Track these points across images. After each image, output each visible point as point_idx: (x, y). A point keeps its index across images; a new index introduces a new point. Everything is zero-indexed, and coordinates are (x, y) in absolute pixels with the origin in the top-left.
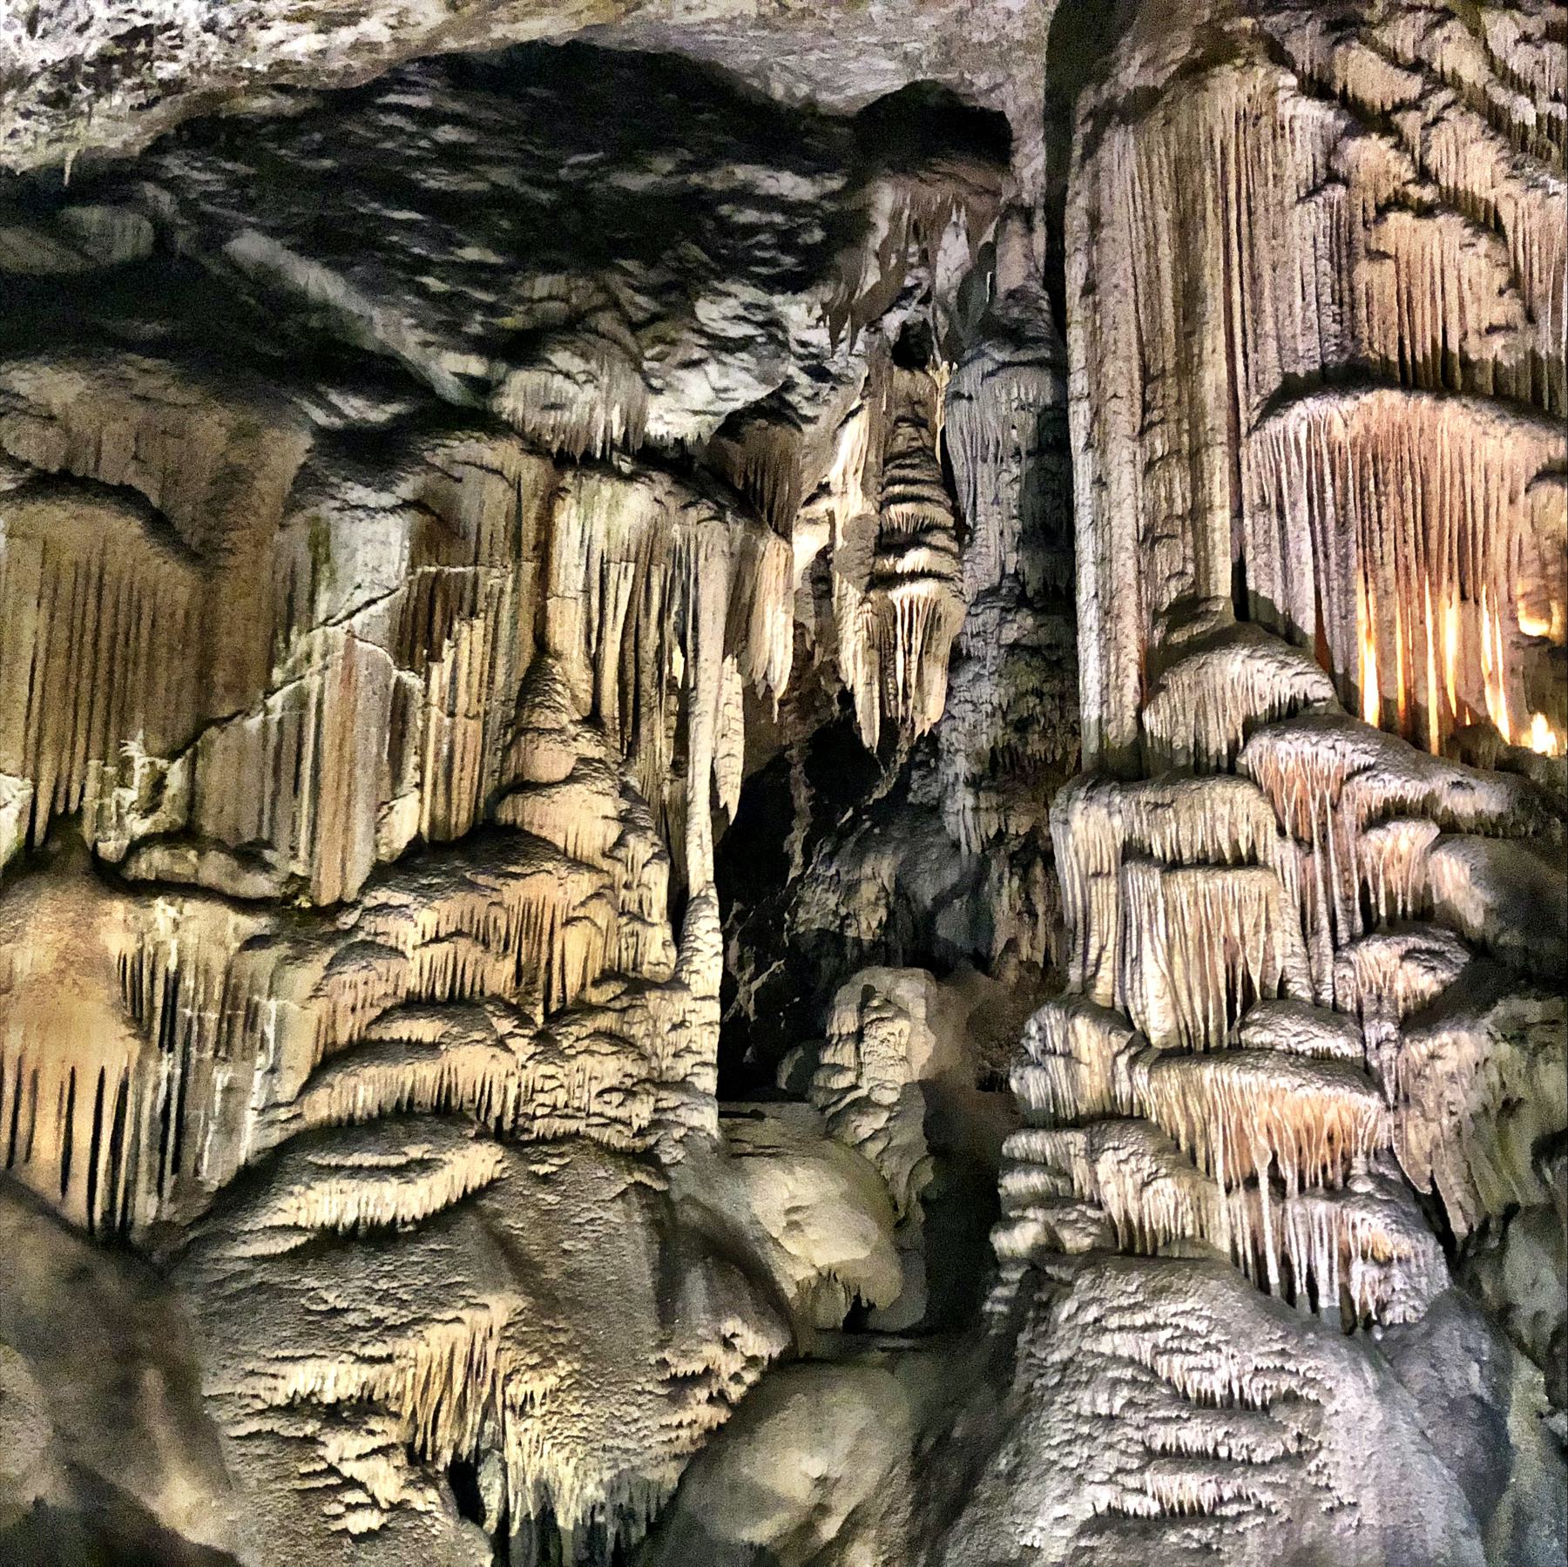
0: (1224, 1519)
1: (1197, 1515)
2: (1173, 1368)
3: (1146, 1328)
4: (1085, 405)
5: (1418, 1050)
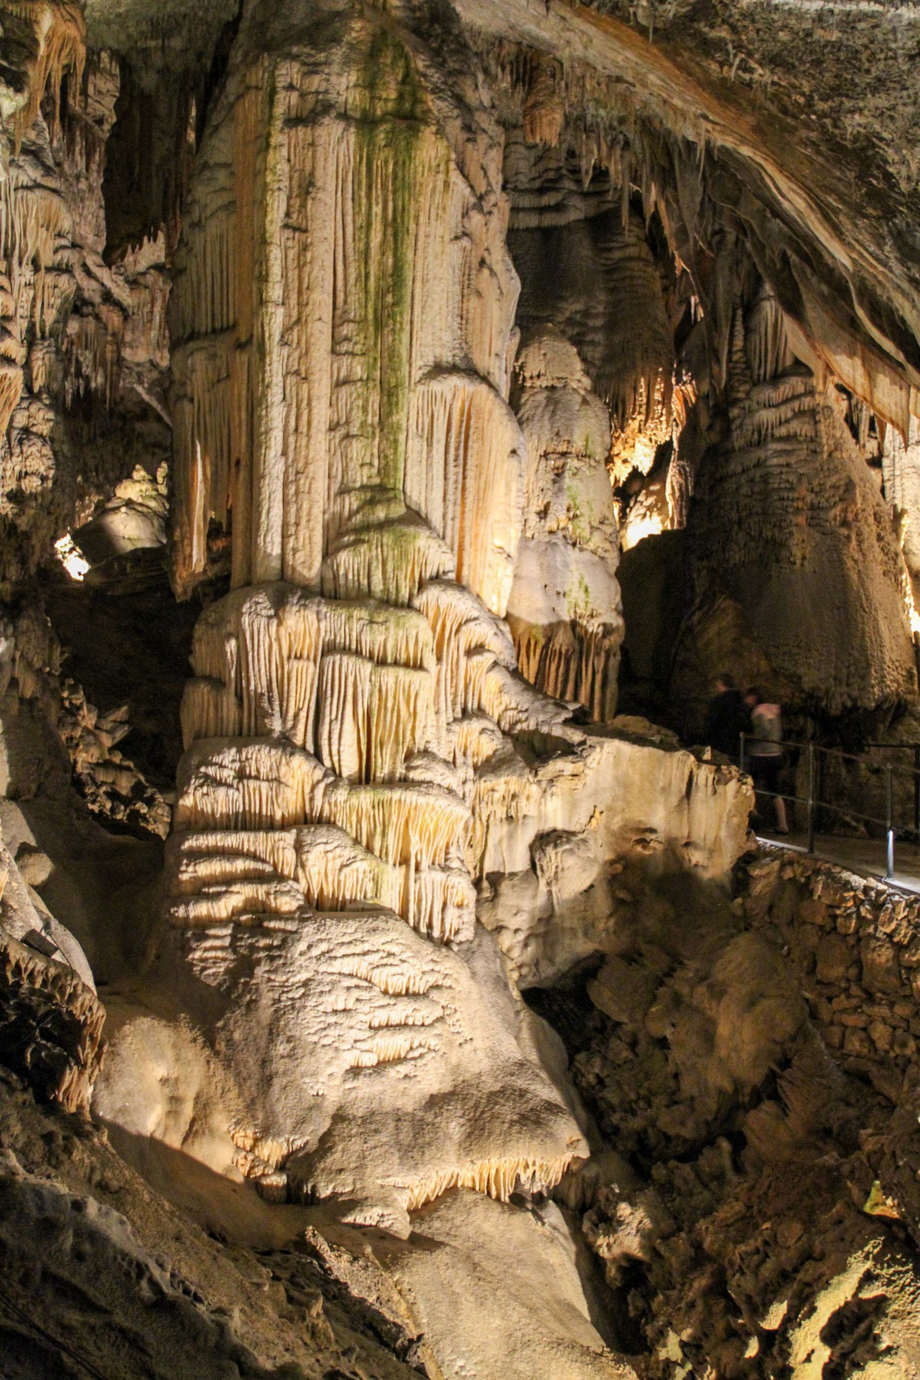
0: (414, 1059)
1: (400, 1060)
2: (380, 977)
3: (365, 954)
4: (281, 311)
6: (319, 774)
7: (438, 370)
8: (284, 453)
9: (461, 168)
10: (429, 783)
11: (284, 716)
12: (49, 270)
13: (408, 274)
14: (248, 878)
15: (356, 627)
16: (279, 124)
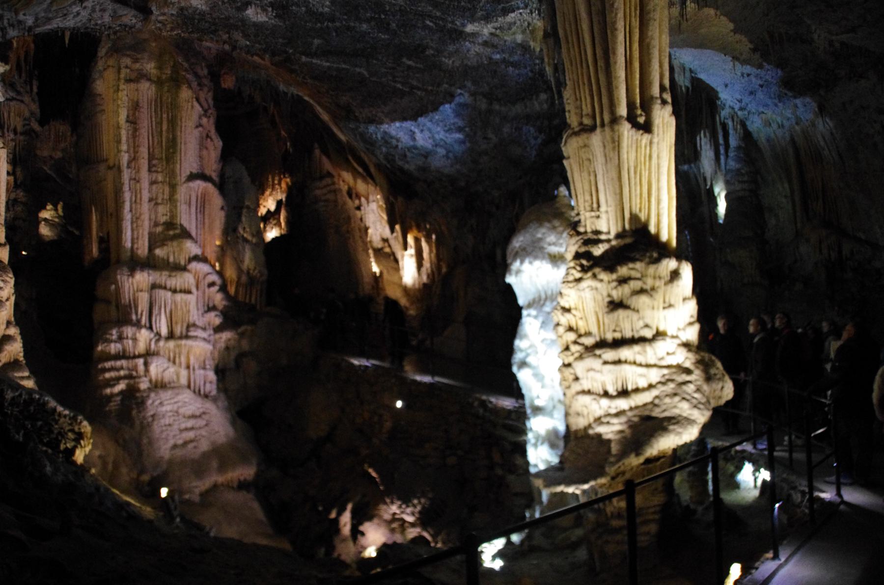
1: (191, 441)
3: (176, 403)
4: (127, 155)
5: (218, 336)
6: (152, 335)
7: (192, 177)
8: (131, 211)
9: (198, 100)
10: (196, 337)
11: (137, 314)
12: (21, 134)
13: (179, 141)
14: (125, 377)
15: (164, 278)
16: (123, 81)
